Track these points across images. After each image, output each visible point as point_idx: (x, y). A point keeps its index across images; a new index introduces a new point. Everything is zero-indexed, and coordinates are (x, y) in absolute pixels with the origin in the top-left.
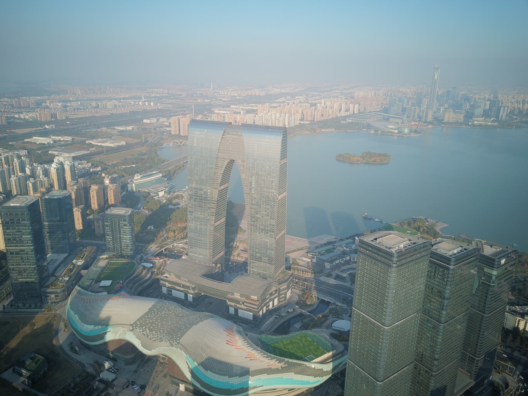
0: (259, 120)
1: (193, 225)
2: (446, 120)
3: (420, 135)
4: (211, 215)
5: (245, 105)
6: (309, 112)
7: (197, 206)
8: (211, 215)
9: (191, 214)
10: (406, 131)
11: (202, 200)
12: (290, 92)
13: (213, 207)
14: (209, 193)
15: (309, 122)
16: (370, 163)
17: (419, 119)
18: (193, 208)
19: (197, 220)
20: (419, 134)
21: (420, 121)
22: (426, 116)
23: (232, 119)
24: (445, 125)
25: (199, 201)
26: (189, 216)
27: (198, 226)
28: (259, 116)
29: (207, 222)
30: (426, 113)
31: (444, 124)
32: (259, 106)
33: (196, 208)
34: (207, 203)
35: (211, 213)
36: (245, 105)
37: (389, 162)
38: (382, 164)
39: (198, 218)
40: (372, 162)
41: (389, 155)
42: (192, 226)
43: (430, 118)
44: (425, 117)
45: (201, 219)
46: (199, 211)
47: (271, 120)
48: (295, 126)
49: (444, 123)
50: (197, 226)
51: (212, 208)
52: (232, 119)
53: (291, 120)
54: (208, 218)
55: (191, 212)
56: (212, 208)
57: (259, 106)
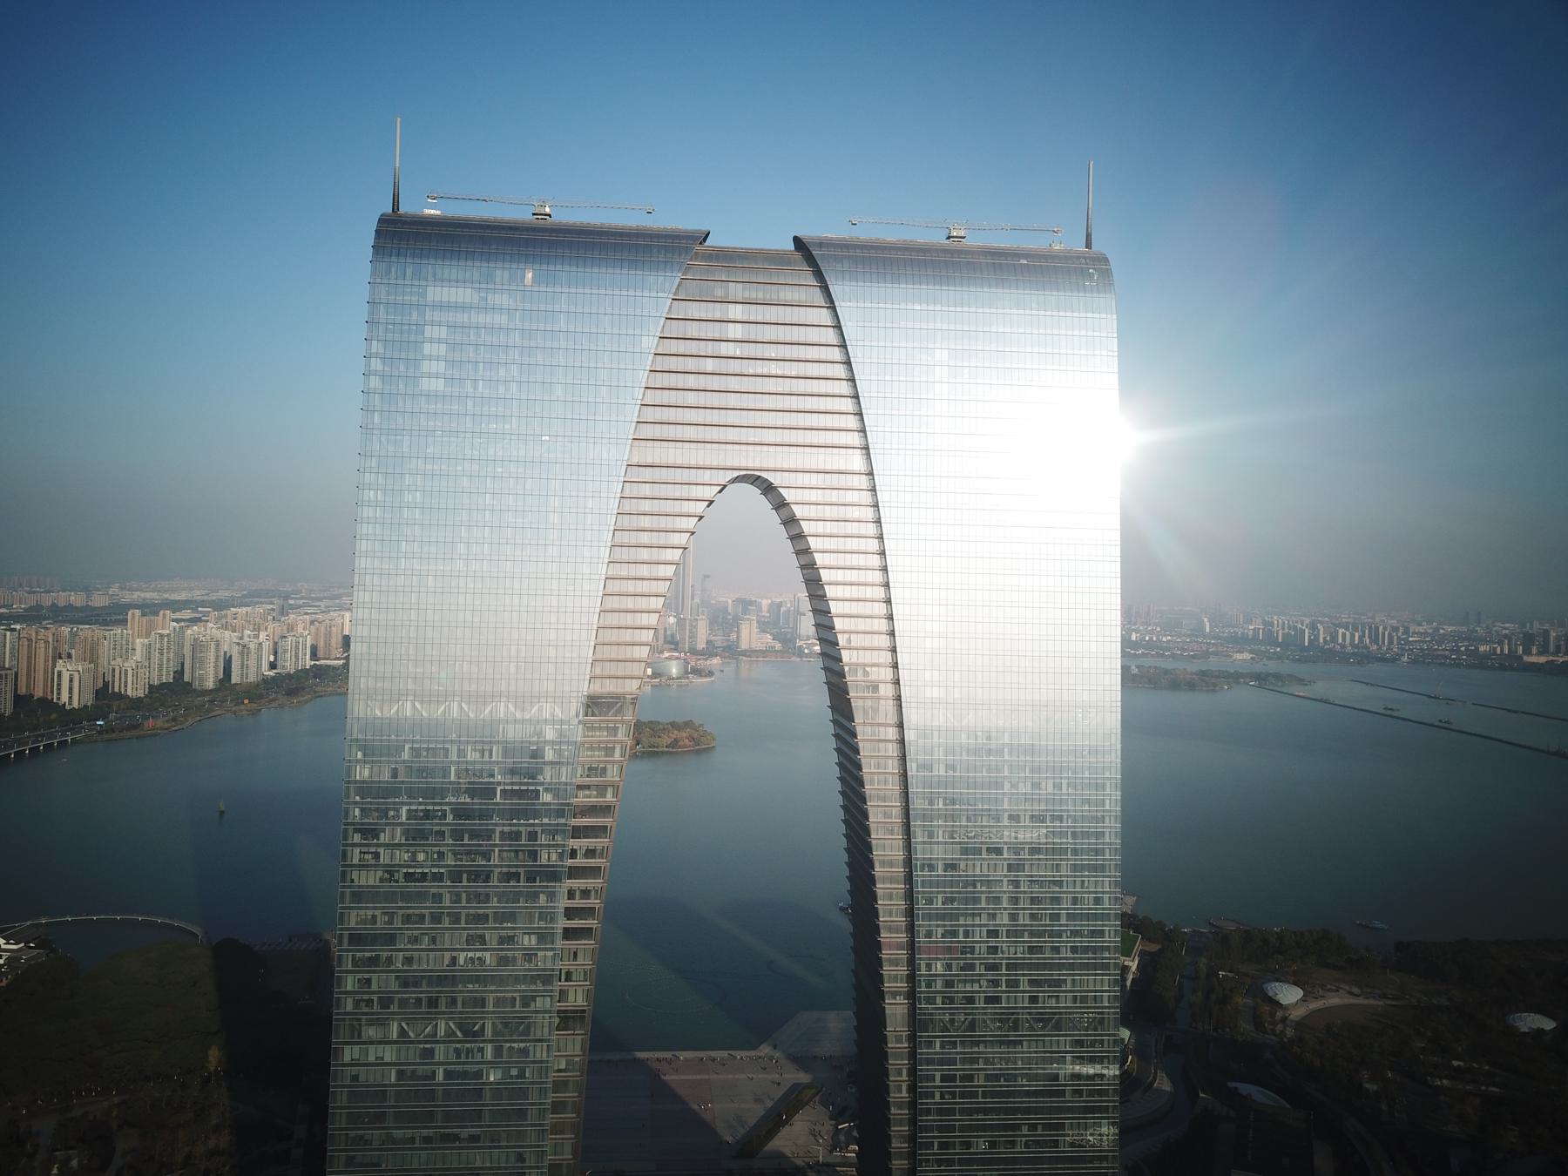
0: (161, 649)
1: (389, 1054)
2: (744, 646)
3: (713, 679)
4: (569, 933)
5: (48, 626)
6: (334, 629)
7: (438, 877)
8: (569, 933)
9: (374, 961)
10: (674, 669)
11: (485, 815)
12: (199, 597)
13: (580, 861)
14: (549, 755)
15: (342, 662)
16: (662, 752)
17: (673, 647)
18: (390, 897)
19: (433, 1003)
20: (710, 676)
21: (676, 650)
22: (693, 636)
23: (47, 642)
24: (749, 656)
25: (457, 835)
26: (350, 983)
27: (440, 1055)
28: (161, 636)
29: (527, 1000)
30: (691, 625)
31: (745, 656)
32: (133, 614)
33: (421, 896)
34: (533, 836)
35: (570, 913)
36: (48, 626)
37: (714, 747)
38: (698, 752)
39: (441, 980)
40: (667, 749)
41: (702, 725)
42: (380, 1063)
43: (701, 645)
44: (690, 638)
45: (477, 980)
46: (456, 918)
47: (213, 646)
48: (298, 671)
49: (745, 653)
50: (429, 1053)
51: (575, 872)
52: (47, 642)
53: (285, 651)
54: (544, 961)
55: (374, 939)
56: (575, 872)
57: (133, 614)
